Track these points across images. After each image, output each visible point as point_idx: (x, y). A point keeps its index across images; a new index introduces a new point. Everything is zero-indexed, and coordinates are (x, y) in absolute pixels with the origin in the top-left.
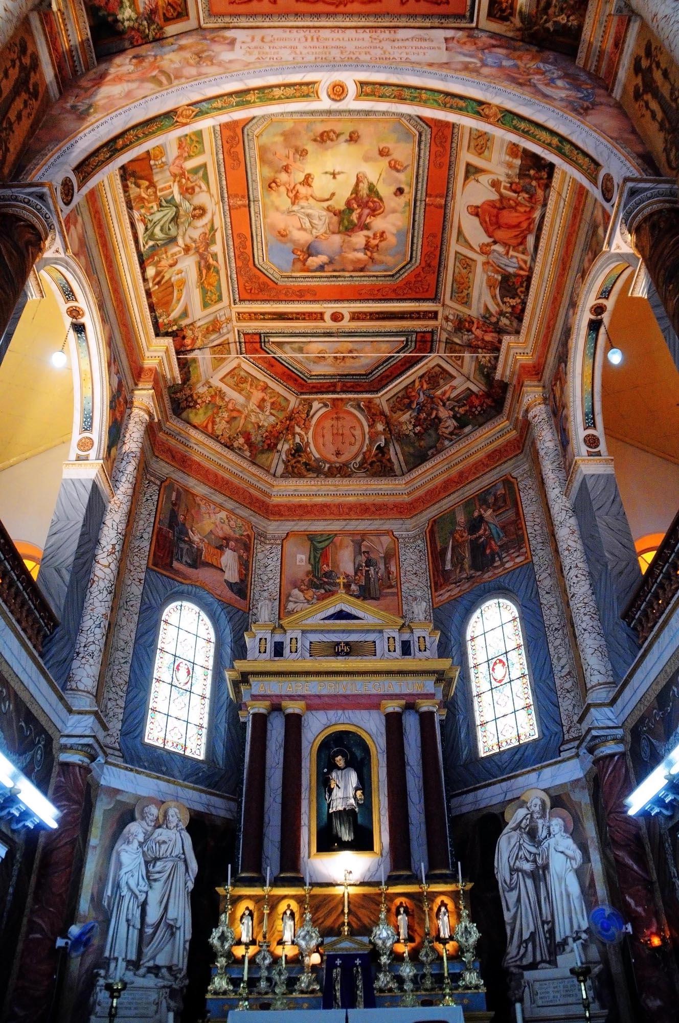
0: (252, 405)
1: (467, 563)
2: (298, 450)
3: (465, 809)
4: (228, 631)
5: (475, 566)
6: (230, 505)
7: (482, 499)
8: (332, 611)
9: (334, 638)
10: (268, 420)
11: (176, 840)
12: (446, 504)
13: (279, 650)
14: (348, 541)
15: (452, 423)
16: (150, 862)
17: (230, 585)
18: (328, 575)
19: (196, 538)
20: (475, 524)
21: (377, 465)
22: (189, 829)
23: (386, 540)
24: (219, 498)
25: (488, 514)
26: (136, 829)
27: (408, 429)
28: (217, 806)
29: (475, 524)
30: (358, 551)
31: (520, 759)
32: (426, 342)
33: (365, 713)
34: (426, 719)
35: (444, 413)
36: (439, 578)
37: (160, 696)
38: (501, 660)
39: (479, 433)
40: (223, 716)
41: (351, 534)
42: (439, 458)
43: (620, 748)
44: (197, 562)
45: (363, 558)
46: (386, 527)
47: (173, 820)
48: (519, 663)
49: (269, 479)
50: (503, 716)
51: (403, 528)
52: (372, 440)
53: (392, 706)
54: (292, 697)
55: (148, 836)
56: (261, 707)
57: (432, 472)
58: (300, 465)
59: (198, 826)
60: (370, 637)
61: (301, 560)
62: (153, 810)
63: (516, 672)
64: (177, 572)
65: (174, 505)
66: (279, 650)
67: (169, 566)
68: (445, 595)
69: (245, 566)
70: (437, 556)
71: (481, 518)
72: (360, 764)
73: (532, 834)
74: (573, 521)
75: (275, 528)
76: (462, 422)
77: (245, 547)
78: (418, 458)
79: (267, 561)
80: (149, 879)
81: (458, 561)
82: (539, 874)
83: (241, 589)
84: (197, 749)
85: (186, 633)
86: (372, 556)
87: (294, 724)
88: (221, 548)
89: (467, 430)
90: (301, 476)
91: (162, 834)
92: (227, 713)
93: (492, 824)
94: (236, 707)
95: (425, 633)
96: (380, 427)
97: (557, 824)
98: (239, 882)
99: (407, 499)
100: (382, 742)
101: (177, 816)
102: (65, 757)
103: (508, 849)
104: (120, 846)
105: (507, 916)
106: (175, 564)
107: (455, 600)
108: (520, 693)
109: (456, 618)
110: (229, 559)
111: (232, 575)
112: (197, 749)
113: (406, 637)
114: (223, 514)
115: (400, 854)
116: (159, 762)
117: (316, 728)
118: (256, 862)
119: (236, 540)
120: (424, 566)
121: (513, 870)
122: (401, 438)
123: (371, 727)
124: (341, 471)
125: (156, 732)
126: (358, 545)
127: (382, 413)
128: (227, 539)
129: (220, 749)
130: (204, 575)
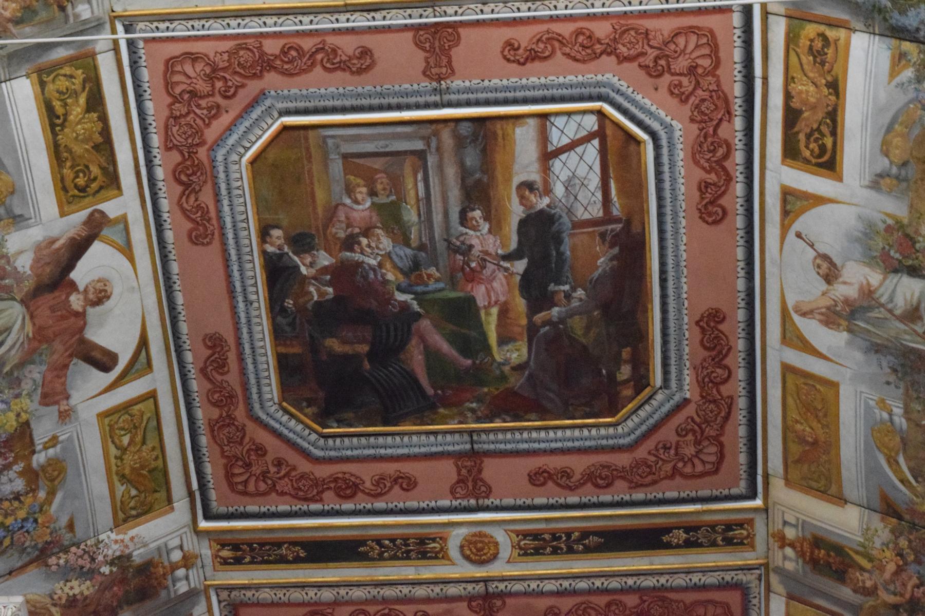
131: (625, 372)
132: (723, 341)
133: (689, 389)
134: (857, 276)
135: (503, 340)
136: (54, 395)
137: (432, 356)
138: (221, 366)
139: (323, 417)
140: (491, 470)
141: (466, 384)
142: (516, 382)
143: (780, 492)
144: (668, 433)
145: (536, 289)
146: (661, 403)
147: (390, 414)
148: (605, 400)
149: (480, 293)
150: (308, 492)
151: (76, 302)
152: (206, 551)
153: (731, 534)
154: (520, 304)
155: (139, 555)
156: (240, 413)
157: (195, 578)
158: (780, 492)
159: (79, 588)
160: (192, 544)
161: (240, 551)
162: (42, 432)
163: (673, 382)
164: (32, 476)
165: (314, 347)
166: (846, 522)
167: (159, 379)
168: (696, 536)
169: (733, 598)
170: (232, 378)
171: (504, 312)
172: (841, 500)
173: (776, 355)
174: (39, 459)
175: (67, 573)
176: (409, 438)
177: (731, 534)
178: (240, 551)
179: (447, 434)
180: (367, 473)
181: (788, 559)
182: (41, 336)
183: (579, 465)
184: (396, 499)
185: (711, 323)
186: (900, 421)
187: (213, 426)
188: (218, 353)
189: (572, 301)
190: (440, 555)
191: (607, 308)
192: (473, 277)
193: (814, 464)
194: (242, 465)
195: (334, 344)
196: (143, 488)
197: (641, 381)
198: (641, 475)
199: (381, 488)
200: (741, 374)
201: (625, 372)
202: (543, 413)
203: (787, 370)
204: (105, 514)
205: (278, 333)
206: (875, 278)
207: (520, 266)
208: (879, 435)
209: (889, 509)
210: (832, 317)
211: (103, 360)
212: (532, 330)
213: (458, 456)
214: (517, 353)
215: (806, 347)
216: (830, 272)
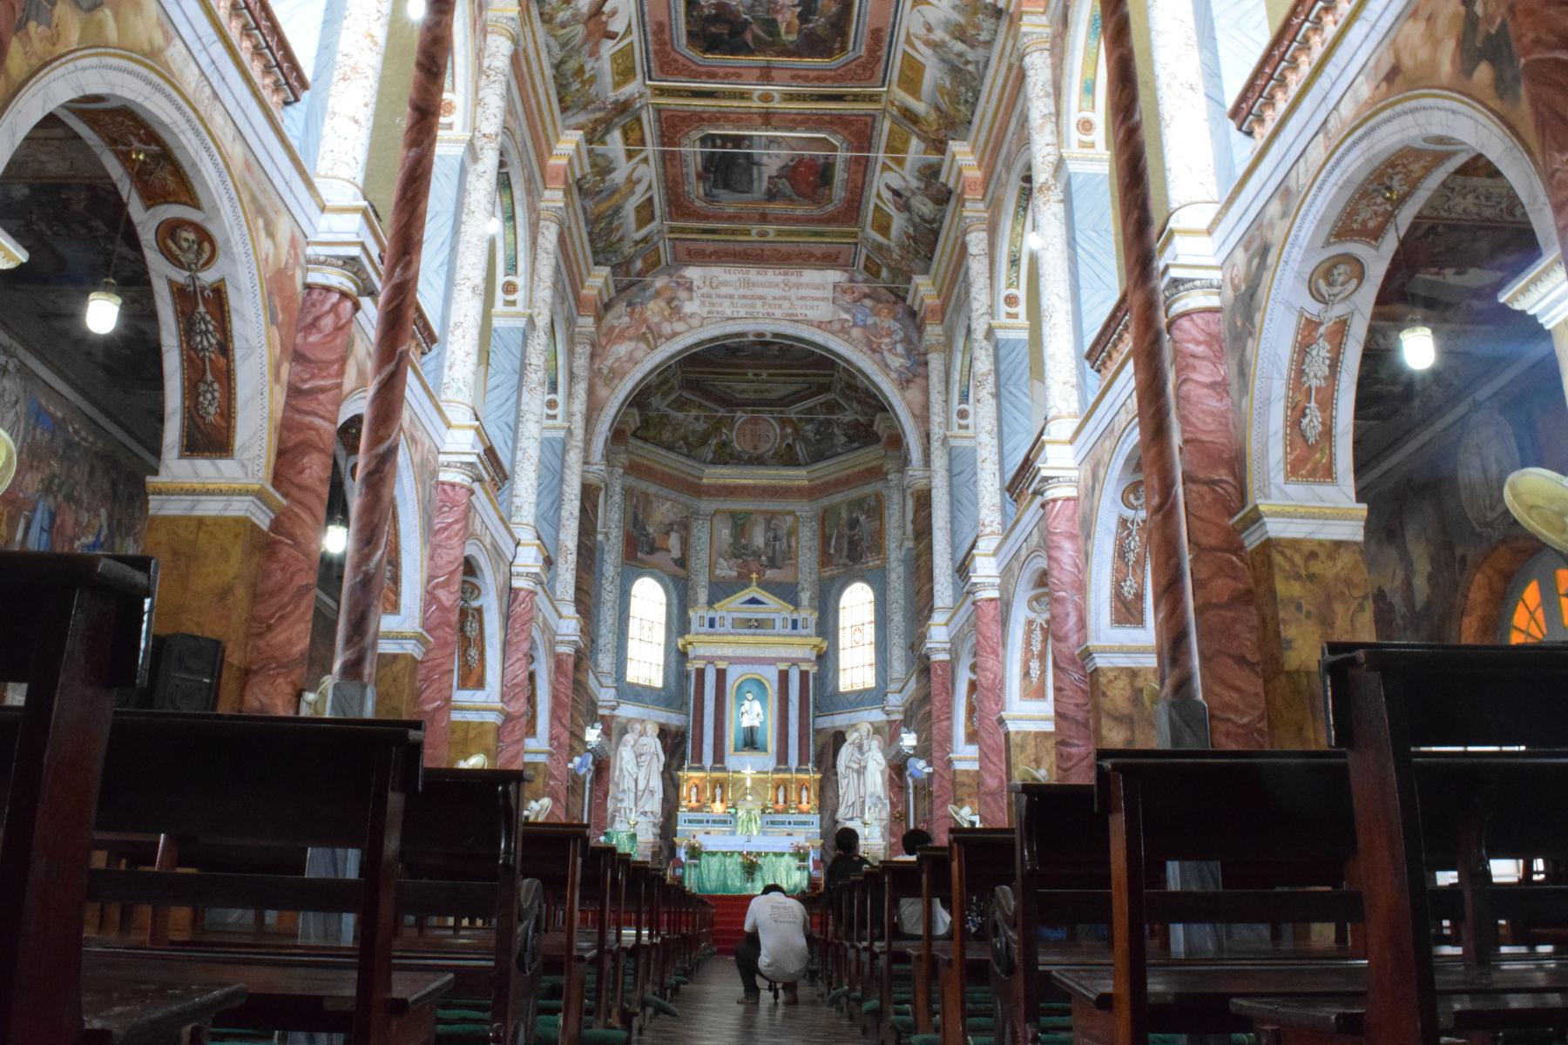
0: (690, 419)
1: (845, 553)
2: (724, 445)
3: (827, 725)
4: (674, 596)
5: (850, 557)
6: (673, 494)
7: (859, 503)
8: (747, 598)
9: (748, 616)
10: (701, 427)
11: (653, 744)
12: (837, 498)
13: (712, 623)
14: (761, 519)
15: (843, 439)
16: (638, 756)
17: (676, 561)
18: (745, 547)
19: (651, 530)
20: (853, 524)
21: (788, 459)
22: (659, 736)
23: (789, 519)
24: (664, 492)
25: (862, 518)
26: (629, 738)
27: (811, 435)
28: (674, 719)
29: (853, 524)
30: (768, 528)
31: (861, 699)
32: (824, 388)
33: (765, 668)
34: (804, 675)
35: (837, 431)
36: (825, 559)
37: (633, 648)
38: (857, 628)
39: (861, 451)
40: (674, 658)
41: (765, 513)
42: (833, 461)
43: (901, 717)
44: (653, 550)
45: (771, 534)
46: (790, 508)
47: (649, 732)
48: (869, 633)
49: (701, 466)
50: (856, 667)
51: (804, 508)
52: (784, 437)
53: (783, 666)
54: (722, 658)
55: (636, 742)
56: (700, 664)
57: (828, 470)
58: (725, 456)
59: (663, 732)
60: (772, 616)
61: (725, 533)
62: (638, 727)
63: (867, 641)
64: (641, 561)
65: (636, 507)
66: (712, 623)
67: (635, 558)
68: (828, 572)
69: (685, 543)
70: (825, 540)
71: (857, 520)
72: (762, 695)
73: (860, 748)
74: (901, 569)
75: (707, 505)
76: (851, 440)
77: (685, 526)
78: (818, 457)
79: (700, 533)
80: (638, 765)
81: (838, 550)
82: (861, 771)
83: (682, 562)
84: (658, 682)
85: (649, 599)
86: (779, 533)
87: (721, 675)
88: (667, 533)
89: (856, 445)
90: (725, 463)
91: (643, 740)
92: (678, 658)
93: (839, 738)
94: (683, 656)
95: (808, 615)
96: (789, 430)
97: (875, 744)
98: (690, 769)
99: (806, 483)
100: (776, 686)
101: (653, 730)
102: (601, 712)
103: (845, 754)
104: (621, 748)
105: (841, 792)
106: (640, 555)
107: (832, 579)
108: (868, 654)
109: (833, 592)
110: (674, 541)
111: (676, 553)
112: (658, 682)
113: (795, 616)
114: (668, 504)
115: (782, 757)
116: (637, 694)
117: (734, 675)
118: (698, 757)
119: (679, 523)
120: (816, 544)
121: (847, 767)
122: (805, 440)
123: (770, 675)
124: (757, 461)
125: (634, 674)
126: (768, 522)
127: (791, 420)
128: (671, 524)
129: (672, 680)
130: (659, 557)
131: (837, 45)
132: (879, 39)
133: (863, 51)
134: (939, 35)
135: (787, 33)
136: (594, 53)
137: (756, 38)
138: (662, 32)
139: (706, 51)
140: (774, 73)
141: (770, 42)
142: (791, 47)
143: (894, 88)
144: (852, 66)
145: (804, 17)
146: (850, 56)
147: (735, 50)
148: (828, 53)
149: (779, 18)
150: (695, 76)
151: (604, 18)
152: (648, 91)
153: (872, 98)
154: (797, 22)
155: (622, 99)
156: (669, 48)
157: (643, 101)
158: (894, 88)
159: (599, 115)
160: (642, 89)
161: (663, 92)
162: (587, 67)
163: (858, 47)
164: (583, 83)
165: (704, 30)
166: (920, 107)
167: (635, 37)
168: (856, 98)
169: (869, 120)
170: (667, 37)
171: (789, 24)
172: (919, 99)
173: (901, 46)
174: (587, 76)
175: (594, 111)
176: (743, 60)
177: (872, 98)
178: (663, 92)
179: (759, 59)
180: (721, 72)
181: (895, 111)
182: (590, 34)
183: (812, 74)
184: (733, 79)
185: (876, 34)
186: (948, 83)
187: (656, 52)
188: (660, 28)
189: (818, 22)
190: (750, 98)
191: (833, 25)
192: (778, 12)
193: (911, 80)
194: (665, 62)
195: (713, 29)
196: (625, 73)
197: (843, 49)
198: (838, 79)
199: (726, 76)
200: (886, 49)
201: (837, 45)
202: (801, 56)
203: (905, 52)
204: (610, 87)
205: (688, 22)
206: (947, 38)
207: (798, 9)
208: (939, 88)
209: (938, 109)
210: (927, 43)
211: (612, 36)
212: (800, 31)
213: (761, 68)
214: (793, 37)
215: (914, 47)
216: (930, 29)
